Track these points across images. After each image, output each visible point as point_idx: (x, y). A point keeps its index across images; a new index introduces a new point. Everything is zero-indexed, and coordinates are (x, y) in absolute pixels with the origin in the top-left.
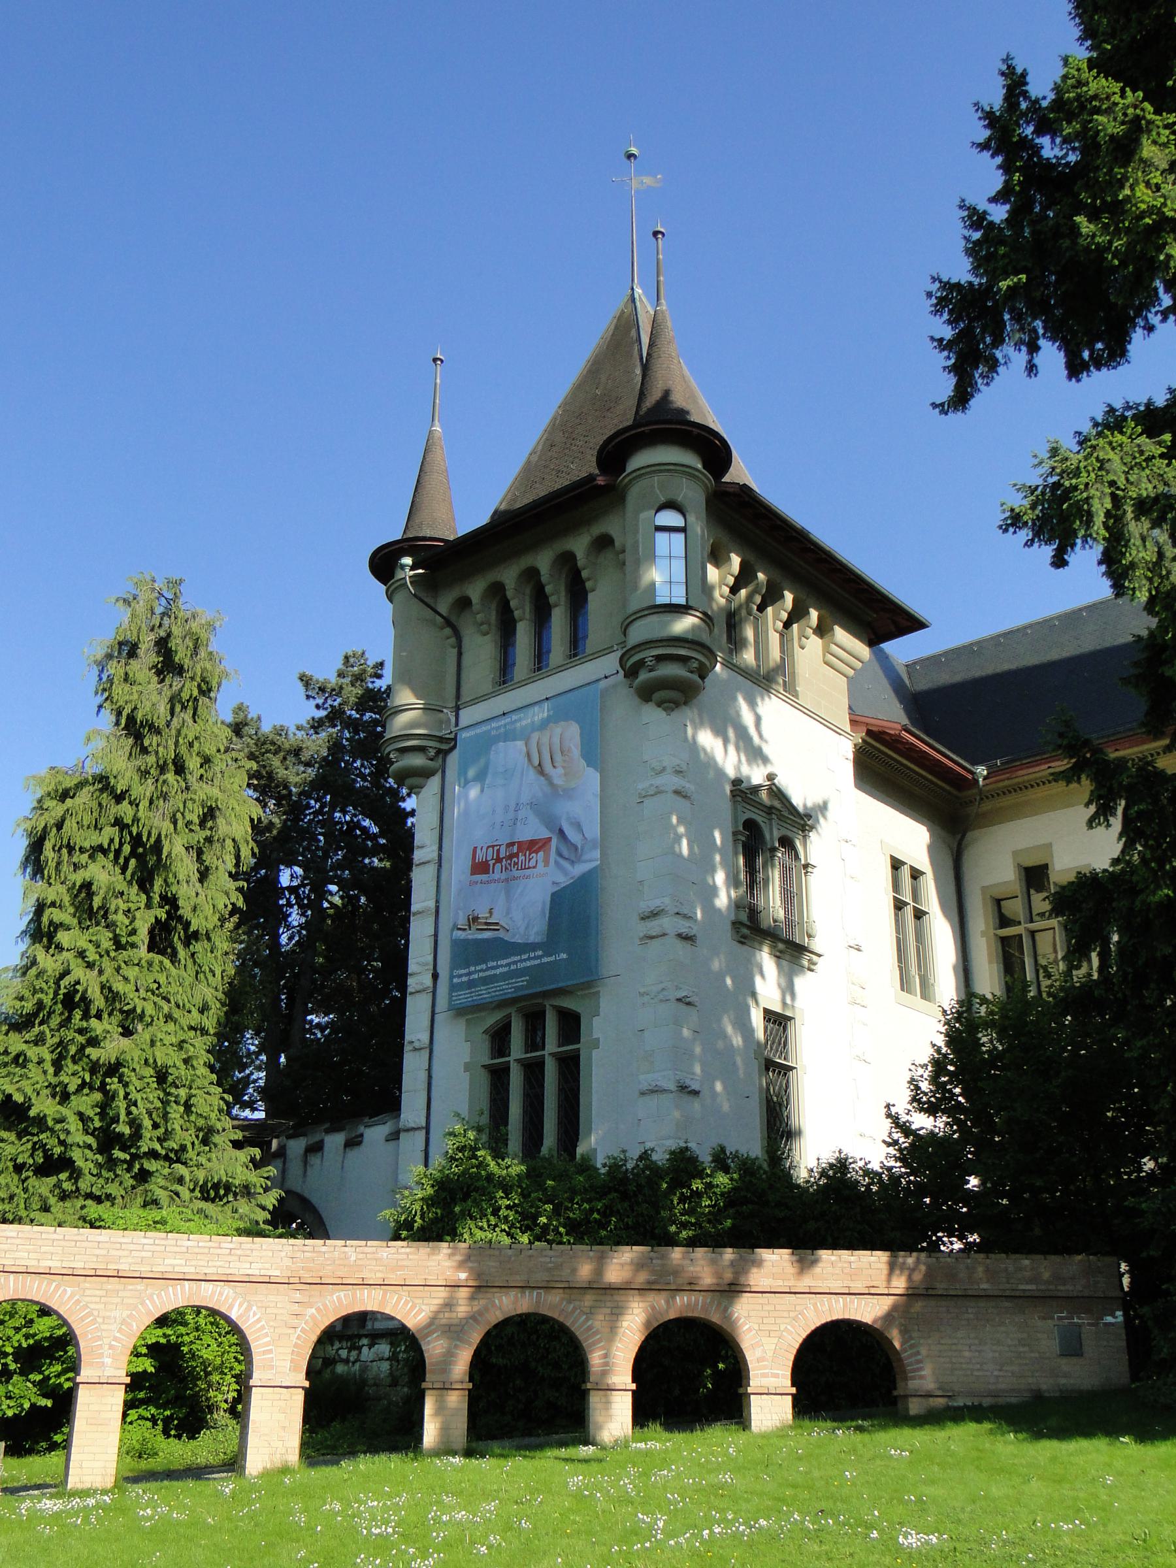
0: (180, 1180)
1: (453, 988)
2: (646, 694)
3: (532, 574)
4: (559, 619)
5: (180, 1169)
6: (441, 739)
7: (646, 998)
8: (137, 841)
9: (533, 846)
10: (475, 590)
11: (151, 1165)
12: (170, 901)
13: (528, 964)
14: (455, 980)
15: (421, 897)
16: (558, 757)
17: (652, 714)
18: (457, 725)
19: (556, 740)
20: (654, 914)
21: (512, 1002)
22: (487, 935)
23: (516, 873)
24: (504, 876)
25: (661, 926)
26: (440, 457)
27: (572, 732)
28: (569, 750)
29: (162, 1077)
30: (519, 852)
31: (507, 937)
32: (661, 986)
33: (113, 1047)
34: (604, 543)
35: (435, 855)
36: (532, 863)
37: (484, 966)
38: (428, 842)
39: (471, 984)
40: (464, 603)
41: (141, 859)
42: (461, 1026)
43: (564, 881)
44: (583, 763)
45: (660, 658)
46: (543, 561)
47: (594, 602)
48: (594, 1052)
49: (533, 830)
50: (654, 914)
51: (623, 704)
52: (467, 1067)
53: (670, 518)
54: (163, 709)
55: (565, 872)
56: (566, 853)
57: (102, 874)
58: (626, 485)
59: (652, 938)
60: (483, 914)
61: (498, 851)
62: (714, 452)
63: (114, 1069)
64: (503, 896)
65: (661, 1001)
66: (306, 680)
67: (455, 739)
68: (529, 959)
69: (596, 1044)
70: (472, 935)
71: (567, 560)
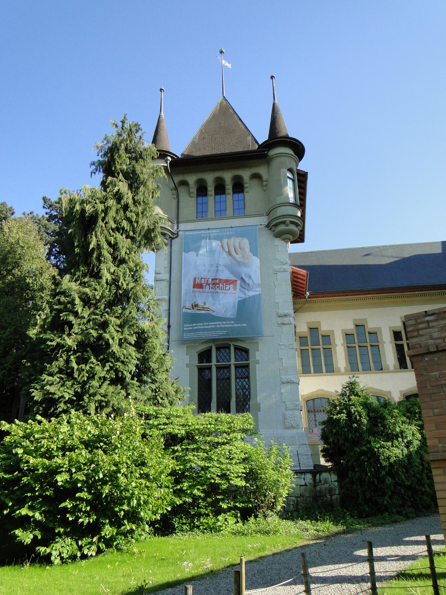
2: (279, 235)
6: (172, 233)
7: (282, 347)
9: (227, 282)
10: (192, 179)
13: (226, 326)
14: (185, 329)
16: (239, 251)
17: (279, 242)
18: (178, 229)
19: (237, 245)
20: (286, 316)
21: (214, 340)
22: (203, 312)
23: (217, 290)
24: (211, 290)
25: (289, 320)
26: (165, 125)
27: (246, 243)
28: (244, 248)
31: (214, 314)
32: (291, 343)
35: (168, 278)
36: (227, 288)
37: (202, 324)
38: (163, 272)
39: (190, 331)
42: (184, 349)
43: (243, 296)
44: (251, 254)
45: (292, 222)
48: (257, 365)
49: (225, 275)
50: (286, 316)
51: (265, 237)
52: (187, 366)
55: (245, 293)
56: (244, 286)
58: (274, 157)
59: (284, 324)
60: (200, 304)
61: (207, 281)
64: (211, 297)
65: (290, 348)
66: (45, 199)
67: (178, 234)
68: (227, 324)
69: (258, 362)
70: (195, 311)
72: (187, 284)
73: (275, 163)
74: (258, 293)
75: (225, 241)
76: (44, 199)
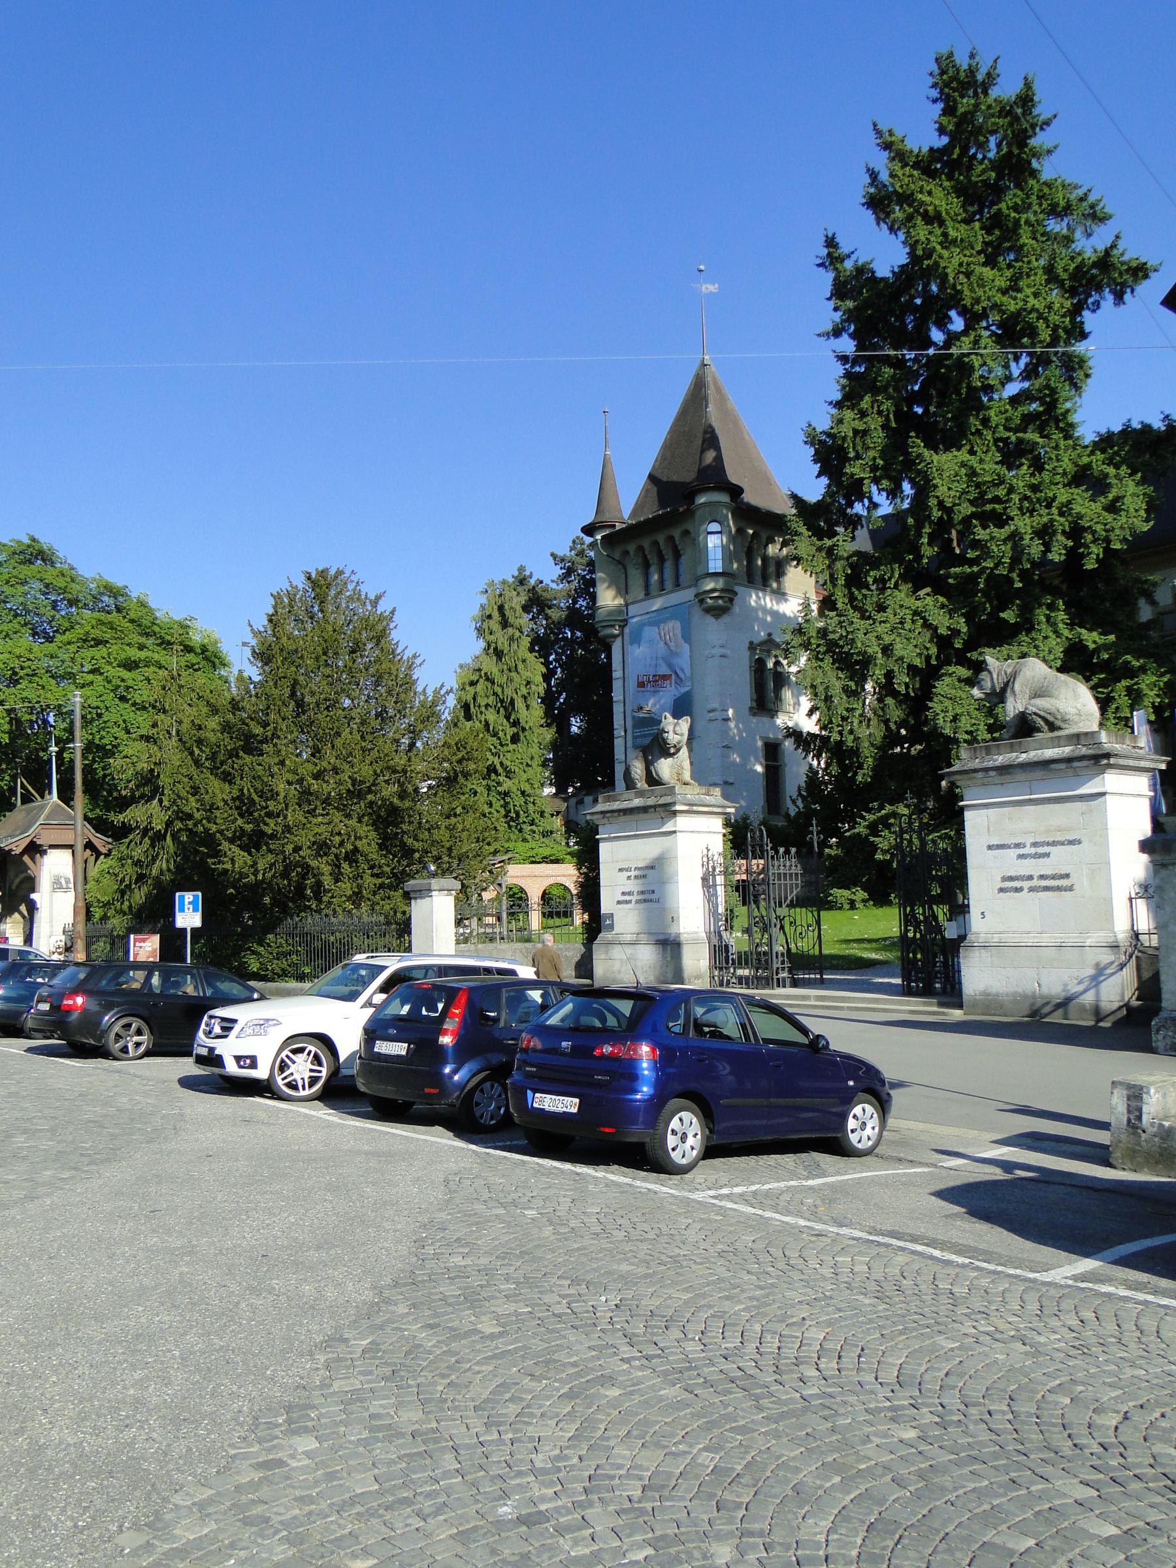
0: (534, 832)
1: (634, 738)
2: (708, 610)
3: (656, 543)
4: (669, 565)
5: (534, 827)
8: (502, 701)
9: (665, 677)
10: (632, 548)
11: (524, 826)
12: (516, 723)
15: (617, 695)
17: (710, 620)
29: (523, 793)
30: (658, 680)
33: (507, 785)
34: (686, 533)
39: (641, 736)
40: (627, 553)
41: (506, 709)
43: (678, 695)
46: (661, 538)
47: (684, 560)
49: (664, 670)
51: (697, 614)
53: (714, 527)
54: (506, 644)
57: (491, 716)
62: (735, 492)
63: (506, 794)
66: (553, 556)
67: (626, 620)
71: (671, 539)
72: (632, 684)
73: (699, 513)
74: (687, 689)
75: (662, 625)
76: (552, 555)
